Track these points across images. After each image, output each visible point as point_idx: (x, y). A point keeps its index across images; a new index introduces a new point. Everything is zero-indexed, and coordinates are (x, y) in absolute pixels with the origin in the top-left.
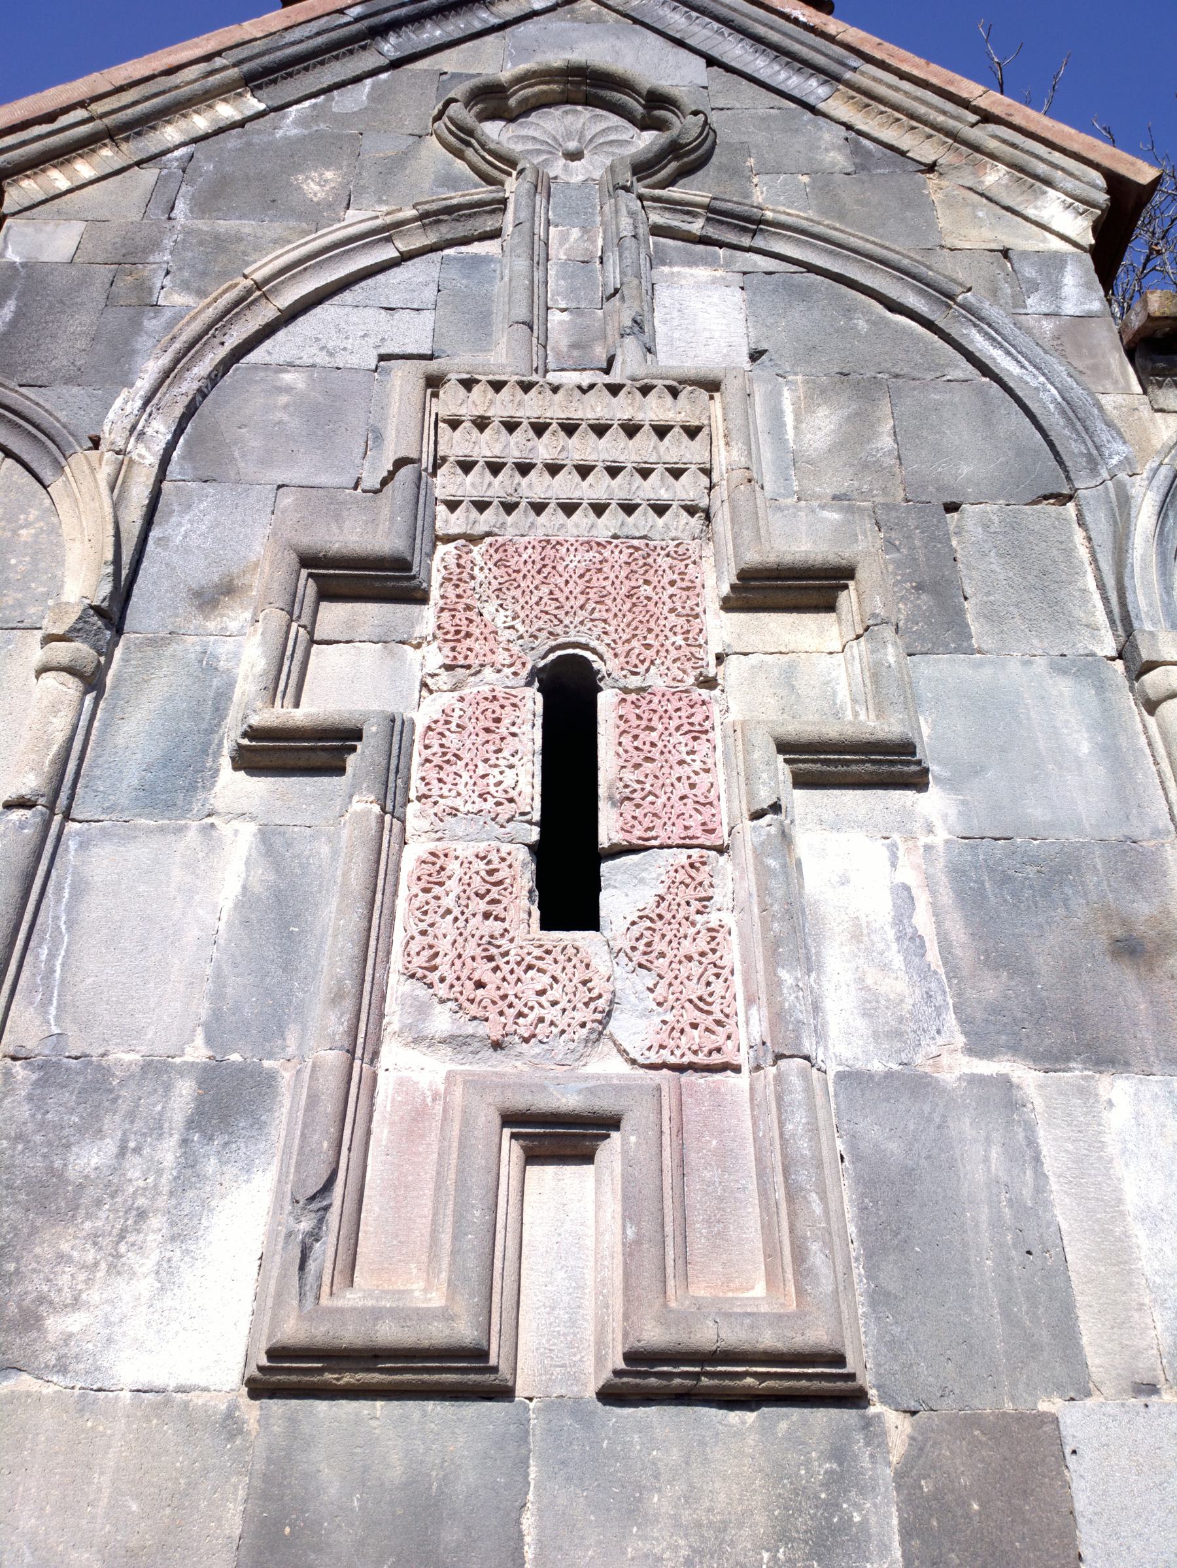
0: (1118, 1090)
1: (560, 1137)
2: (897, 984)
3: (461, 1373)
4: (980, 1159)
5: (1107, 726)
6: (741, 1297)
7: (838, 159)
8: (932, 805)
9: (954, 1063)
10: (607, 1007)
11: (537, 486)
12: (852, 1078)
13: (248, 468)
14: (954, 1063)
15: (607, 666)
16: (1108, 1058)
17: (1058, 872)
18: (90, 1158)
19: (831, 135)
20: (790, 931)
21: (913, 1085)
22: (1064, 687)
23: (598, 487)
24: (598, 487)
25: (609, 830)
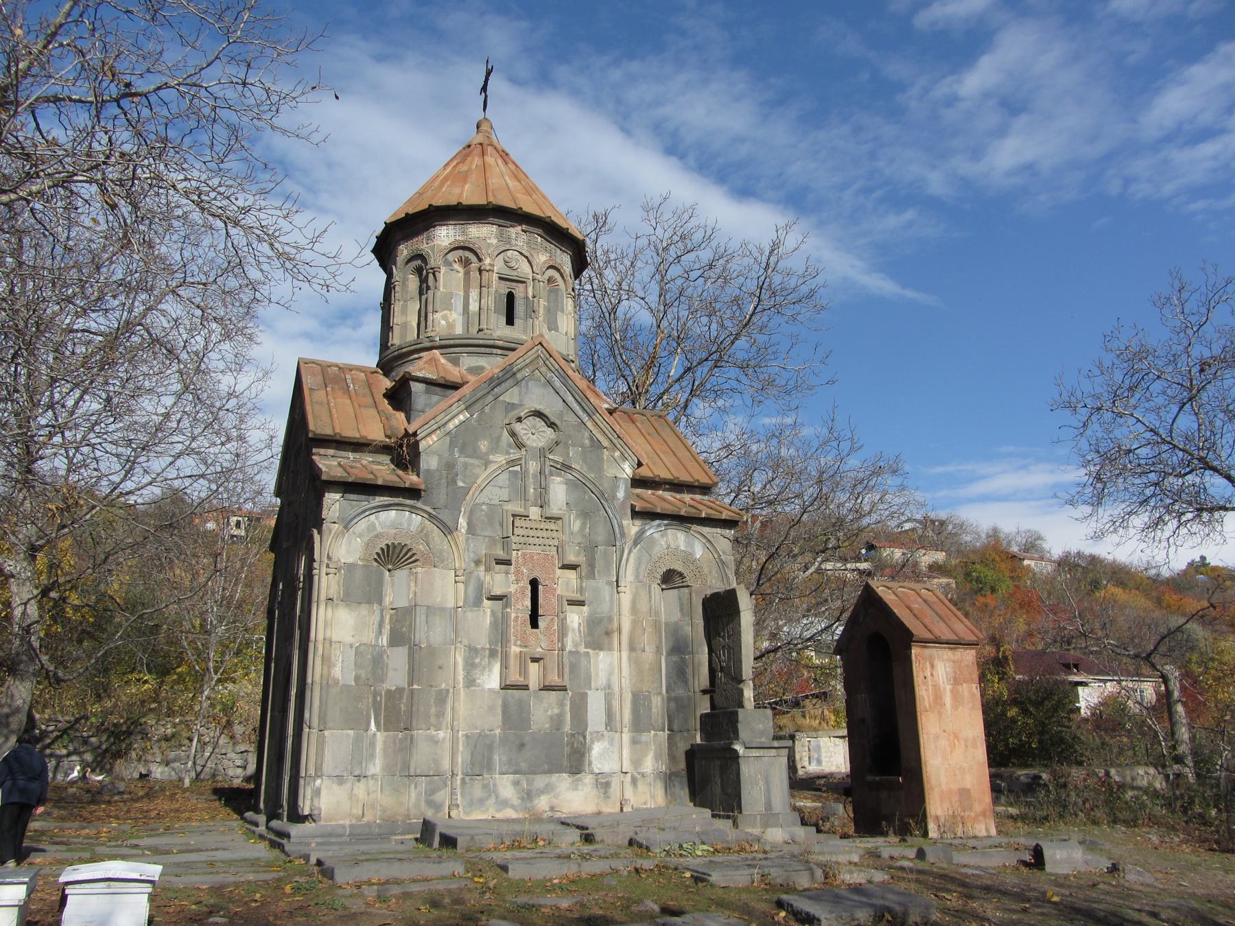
0: (602, 653)
1: (535, 660)
2: (577, 638)
3: (526, 687)
4: (584, 662)
5: (611, 595)
6: (554, 679)
7: (587, 442)
8: (585, 608)
9: (582, 649)
10: (539, 642)
11: (531, 540)
12: (570, 652)
13: (479, 532)
14: (582, 649)
15: (541, 581)
16: (601, 649)
17: (601, 620)
18: (477, 661)
19: (587, 434)
20: (563, 631)
21: (577, 653)
22: (607, 587)
23: (541, 541)
24: (541, 541)
25: (541, 612)
